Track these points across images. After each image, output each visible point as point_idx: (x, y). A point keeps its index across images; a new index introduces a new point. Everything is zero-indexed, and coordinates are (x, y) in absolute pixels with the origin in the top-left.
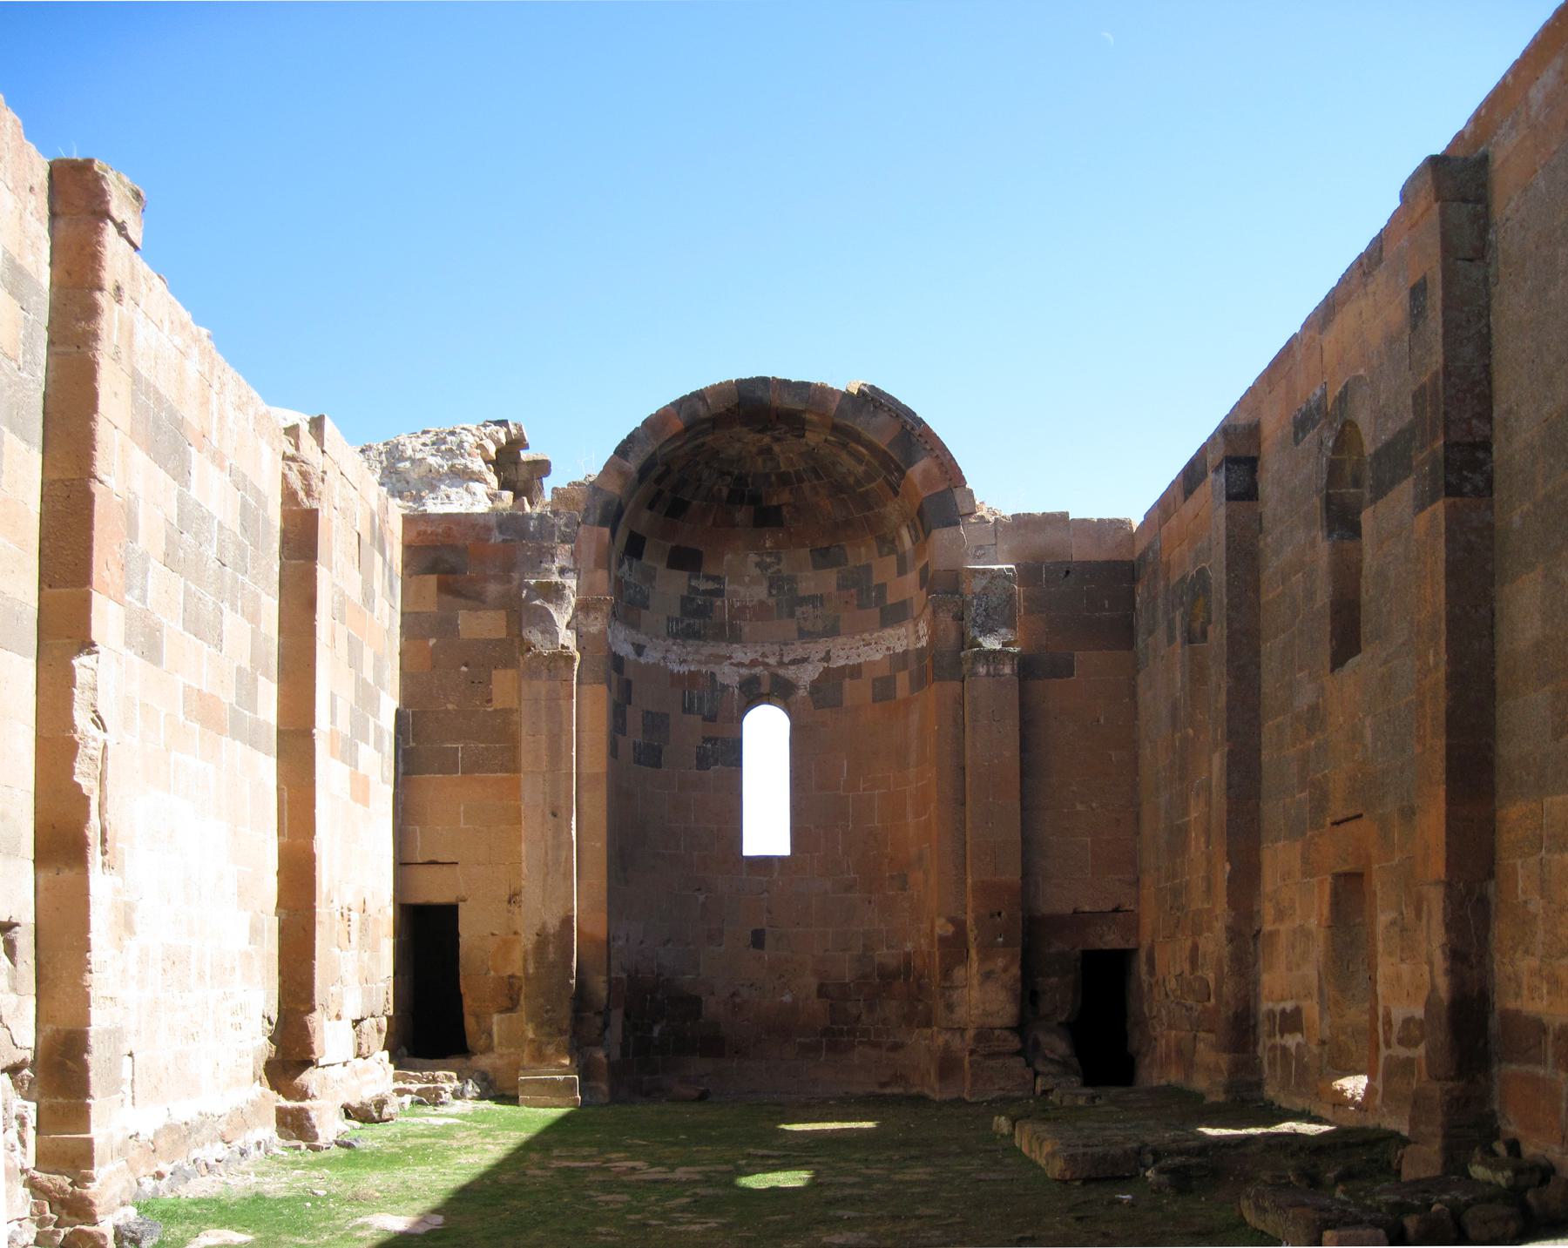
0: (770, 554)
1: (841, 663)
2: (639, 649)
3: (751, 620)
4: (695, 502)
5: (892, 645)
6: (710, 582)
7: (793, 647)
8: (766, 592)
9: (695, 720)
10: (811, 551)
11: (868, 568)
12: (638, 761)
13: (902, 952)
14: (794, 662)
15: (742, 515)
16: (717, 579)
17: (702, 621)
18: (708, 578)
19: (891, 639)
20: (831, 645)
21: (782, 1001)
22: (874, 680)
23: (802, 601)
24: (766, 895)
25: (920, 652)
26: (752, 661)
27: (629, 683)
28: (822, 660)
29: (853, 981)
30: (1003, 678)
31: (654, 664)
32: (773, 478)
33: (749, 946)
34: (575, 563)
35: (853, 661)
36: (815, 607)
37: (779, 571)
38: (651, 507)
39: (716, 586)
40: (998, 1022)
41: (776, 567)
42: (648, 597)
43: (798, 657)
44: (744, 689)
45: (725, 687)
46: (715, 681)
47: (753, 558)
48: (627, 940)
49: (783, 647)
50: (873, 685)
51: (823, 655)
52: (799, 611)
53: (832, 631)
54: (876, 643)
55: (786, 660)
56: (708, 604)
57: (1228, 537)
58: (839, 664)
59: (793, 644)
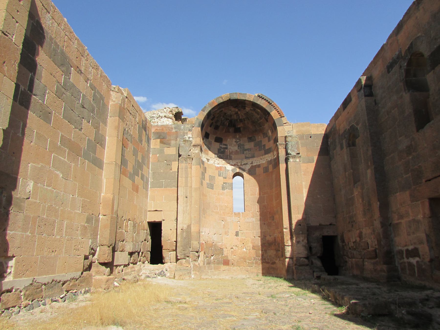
0: (238, 139)
1: (255, 164)
2: (208, 160)
3: (234, 155)
4: (221, 126)
5: (267, 159)
6: (224, 146)
7: (244, 161)
8: (237, 148)
9: (221, 178)
10: (248, 138)
12: (208, 188)
14: (244, 164)
15: (231, 130)
16: (226, 145)
19: (267, 157)
22: (263, 168)
23: (246, 150)
24: (239, 222)
25: (275, 159)
26: (234, 164)
27: (206, 168)
28: (251, 164)
31: (212, 164)
32: (238, 120)
34: (192, 136)
37: (240, 143)
38: (211, 126)
39: (226, 147)
41: (239, 142)
43: (245, 163)
44: (233, 171)
45: (228, 170)
46: (226, 169)
47: (234, 140)
49: (242, 161)
50: (263, 169)
51: (251, 162)
52: (245, 152)
53: (253, 157)
55: (242, 164)
57: (366, 107)
58: (255, 165)
59: (244, 160)
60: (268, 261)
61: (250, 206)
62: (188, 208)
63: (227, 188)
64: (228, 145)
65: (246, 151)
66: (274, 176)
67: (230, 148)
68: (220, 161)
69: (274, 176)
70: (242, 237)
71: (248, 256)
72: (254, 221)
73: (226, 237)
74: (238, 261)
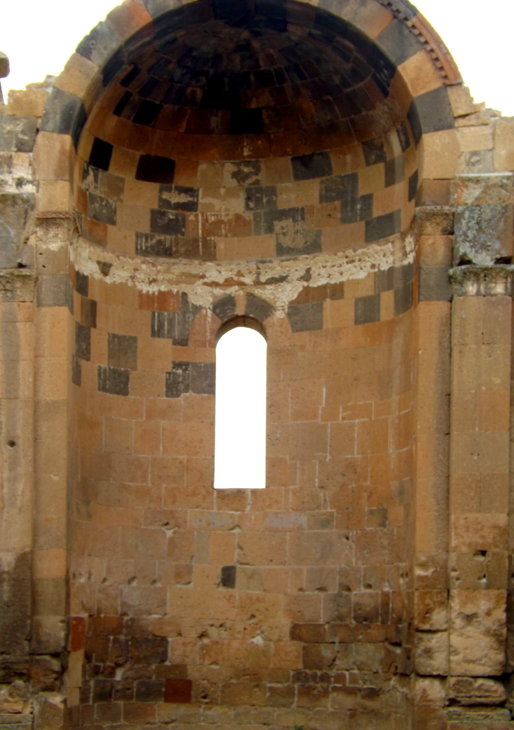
3: (226, 236)
7: (270, 265)
11: (353, 178)
13: (380, 592)
16: (190, 191)
17: (174, 237)
18: (182, 190)
20: (312, 262)
21: (253, 643)
24: (237, 531)
29: (328, 623)
30: (494, 299)
33: (219, 584)
35: (336, 279)
36: (295, 221)
40: (479, 670)
42: (115, 212)
48: (89, 578)
50: (356, 305)
54: (360, 260)
56: (180, 218)
60: (352, 685)
61: (289, 462)
62: (20, 486)
63: (188, 385)
64: (198, 190)
65: (280, 220)
66: (399, 341)
67: (210, 206)
68: (159, 268)
69: (399, 341)
70: (248, 588)
71: (271, 666)
72: (305, 526)
73: (180, 589)
74: (227, 686)
